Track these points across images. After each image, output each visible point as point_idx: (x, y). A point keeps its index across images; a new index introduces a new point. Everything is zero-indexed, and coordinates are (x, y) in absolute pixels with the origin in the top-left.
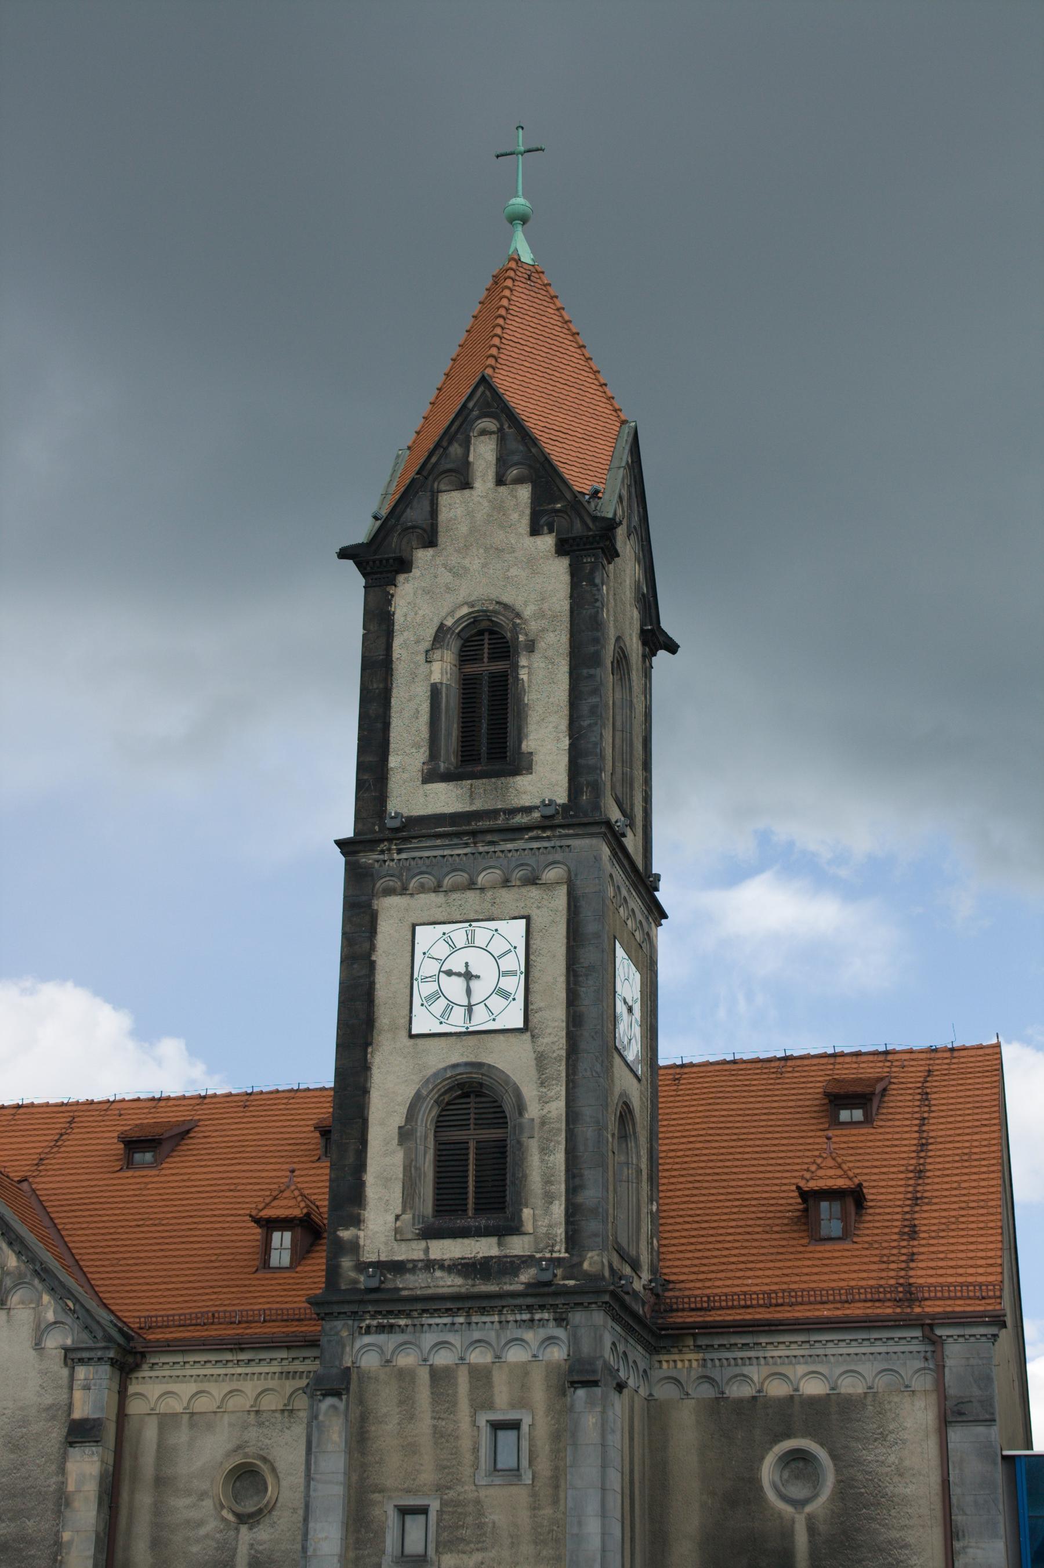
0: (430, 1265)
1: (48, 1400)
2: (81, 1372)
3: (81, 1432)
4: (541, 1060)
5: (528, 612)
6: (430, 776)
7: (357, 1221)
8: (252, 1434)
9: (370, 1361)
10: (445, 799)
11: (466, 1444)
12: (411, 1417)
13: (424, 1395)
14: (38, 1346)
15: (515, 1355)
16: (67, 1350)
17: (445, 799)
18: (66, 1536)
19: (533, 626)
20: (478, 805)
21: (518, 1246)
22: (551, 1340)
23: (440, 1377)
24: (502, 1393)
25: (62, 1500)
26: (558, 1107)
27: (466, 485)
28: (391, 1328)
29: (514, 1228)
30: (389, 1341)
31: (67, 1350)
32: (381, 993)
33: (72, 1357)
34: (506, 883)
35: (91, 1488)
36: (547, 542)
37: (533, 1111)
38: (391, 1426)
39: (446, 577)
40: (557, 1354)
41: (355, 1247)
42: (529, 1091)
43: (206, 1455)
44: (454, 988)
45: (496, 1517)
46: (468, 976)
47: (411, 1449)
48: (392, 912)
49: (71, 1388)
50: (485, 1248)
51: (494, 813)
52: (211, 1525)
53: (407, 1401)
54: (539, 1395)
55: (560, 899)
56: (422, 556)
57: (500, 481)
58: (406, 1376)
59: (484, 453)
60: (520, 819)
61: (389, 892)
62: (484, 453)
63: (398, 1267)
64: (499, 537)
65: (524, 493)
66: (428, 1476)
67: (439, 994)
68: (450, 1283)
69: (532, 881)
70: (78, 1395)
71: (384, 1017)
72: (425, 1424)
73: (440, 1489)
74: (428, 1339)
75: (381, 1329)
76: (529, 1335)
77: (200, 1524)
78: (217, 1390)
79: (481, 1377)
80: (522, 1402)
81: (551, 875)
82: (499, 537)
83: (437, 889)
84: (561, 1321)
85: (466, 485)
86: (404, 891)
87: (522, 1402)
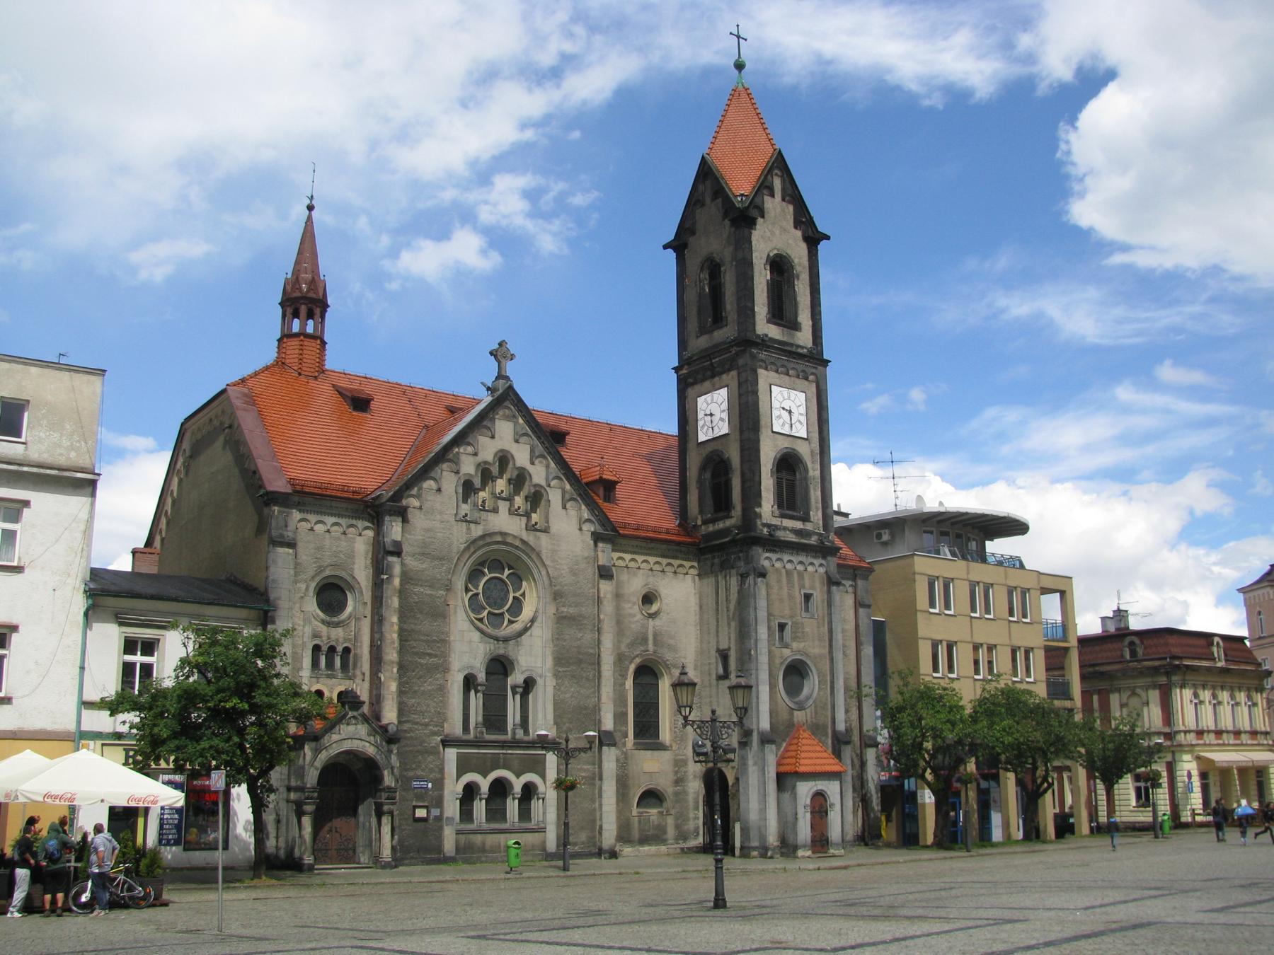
0: (785, 529)
1: (586, 554)
2: (600, 545)
3: (605, 573)
4: (812, 452)
5: (796, 261)
6: (769, 321)
7: (760, 505)
8: (651, 579)
9: (766, 564)
10: (774, 332)
11: (798, 601)
12: (781, 588)
13: (784, 580)
14: (580, 529)
15: (810, 569)
16: (593, 533)
17: (774, 332)
18: (602, 617)
19: (798, 269)
20: (785, 339)
21: (809, 526)
22: (821, 565)
23: (788, 573)
24: (807, 583)
25: (599, 600)
26: (818, 473)
27: (773, 196)
28: (773, 551)
29: (806, 519)
30: (774, 556)
31: (593, 533)
32: (761, 410)
33: (597, 538)
34: (798, 377)
35: (609, 596)
36: (799, 233)
37: (811, 473)
38: (775, 590)
39: (768, 234)
40: (822, 570)
41: (759, 516)
42: (810, 465)
43: (635, 585)
44: (785, 414)
45: (807, 630)
46: (790, 412)
47: (781, 601)
48: (764, 376)
49: (596, 551)
50: (798, 525)
51: (792, 345)
52: (639, 617)
53: (779, 581)
54: (818, 585)
55: (814, 390)
56: (760, 221)
57: (783, 200)
58: (777, 570)
59: (777, 183)
60: (800, 351)
61: (761, 367)
62: (777, 183)
63: (776, 528)
64: (784, 224)
65: (791, 208)
66: (787, 612)
67: (779, 417)
68: (791, 538)
69: (806, 379)
70: (600, 554)
71: (762, 423)
72: (785, 591)
73: (792, 617)
74: (786, 557)
75: (768, 551)
76: (815, 562)
77: (634, 616)
78: (640, 558)
79: (801, 575)
80: (813, 587)
81: (811, 377)
82: (784, 224)
83: (777, 371)
84: (824, 558)
85: (773, 196)
86: (766, 369)
87: (813, 587)
